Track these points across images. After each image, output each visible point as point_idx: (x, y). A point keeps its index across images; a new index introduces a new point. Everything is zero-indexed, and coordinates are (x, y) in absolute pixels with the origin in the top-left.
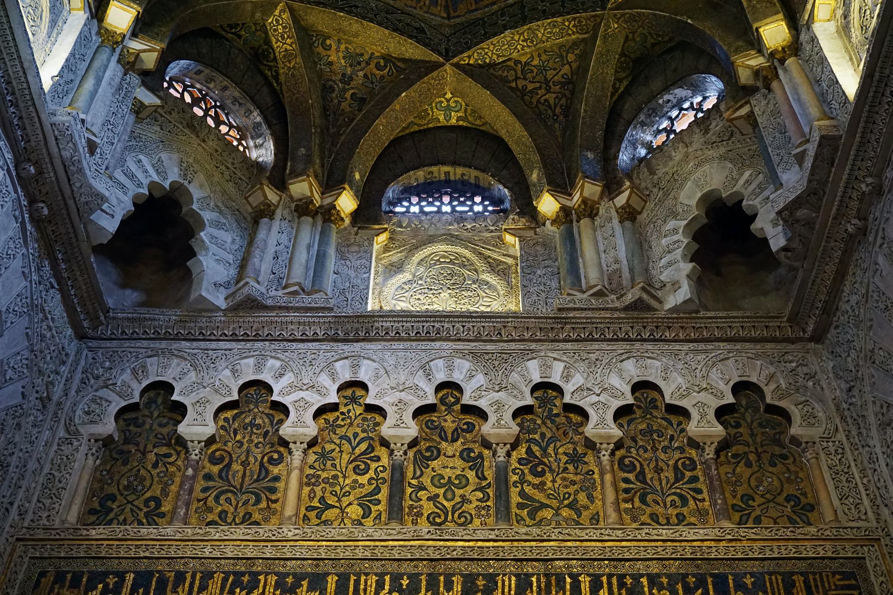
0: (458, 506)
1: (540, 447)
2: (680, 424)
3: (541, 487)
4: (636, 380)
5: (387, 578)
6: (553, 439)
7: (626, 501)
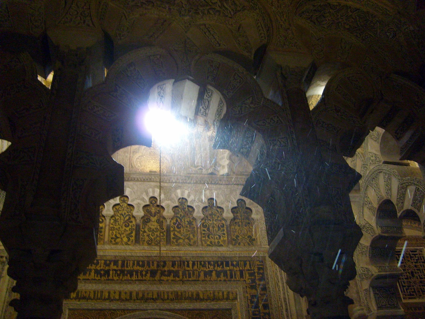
0: (155, 238)
1: (180, 219)
2: (221, 212)
3: (179, 232)
4: (209, 197)
5: (136, 262)
6: (184, 216)
7: (203, 237)
